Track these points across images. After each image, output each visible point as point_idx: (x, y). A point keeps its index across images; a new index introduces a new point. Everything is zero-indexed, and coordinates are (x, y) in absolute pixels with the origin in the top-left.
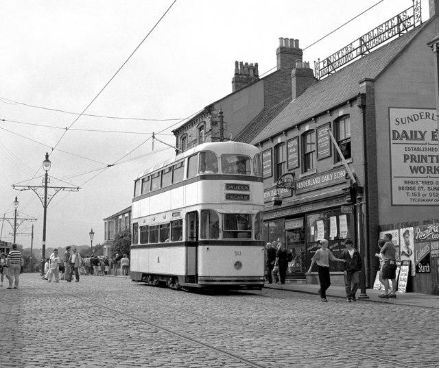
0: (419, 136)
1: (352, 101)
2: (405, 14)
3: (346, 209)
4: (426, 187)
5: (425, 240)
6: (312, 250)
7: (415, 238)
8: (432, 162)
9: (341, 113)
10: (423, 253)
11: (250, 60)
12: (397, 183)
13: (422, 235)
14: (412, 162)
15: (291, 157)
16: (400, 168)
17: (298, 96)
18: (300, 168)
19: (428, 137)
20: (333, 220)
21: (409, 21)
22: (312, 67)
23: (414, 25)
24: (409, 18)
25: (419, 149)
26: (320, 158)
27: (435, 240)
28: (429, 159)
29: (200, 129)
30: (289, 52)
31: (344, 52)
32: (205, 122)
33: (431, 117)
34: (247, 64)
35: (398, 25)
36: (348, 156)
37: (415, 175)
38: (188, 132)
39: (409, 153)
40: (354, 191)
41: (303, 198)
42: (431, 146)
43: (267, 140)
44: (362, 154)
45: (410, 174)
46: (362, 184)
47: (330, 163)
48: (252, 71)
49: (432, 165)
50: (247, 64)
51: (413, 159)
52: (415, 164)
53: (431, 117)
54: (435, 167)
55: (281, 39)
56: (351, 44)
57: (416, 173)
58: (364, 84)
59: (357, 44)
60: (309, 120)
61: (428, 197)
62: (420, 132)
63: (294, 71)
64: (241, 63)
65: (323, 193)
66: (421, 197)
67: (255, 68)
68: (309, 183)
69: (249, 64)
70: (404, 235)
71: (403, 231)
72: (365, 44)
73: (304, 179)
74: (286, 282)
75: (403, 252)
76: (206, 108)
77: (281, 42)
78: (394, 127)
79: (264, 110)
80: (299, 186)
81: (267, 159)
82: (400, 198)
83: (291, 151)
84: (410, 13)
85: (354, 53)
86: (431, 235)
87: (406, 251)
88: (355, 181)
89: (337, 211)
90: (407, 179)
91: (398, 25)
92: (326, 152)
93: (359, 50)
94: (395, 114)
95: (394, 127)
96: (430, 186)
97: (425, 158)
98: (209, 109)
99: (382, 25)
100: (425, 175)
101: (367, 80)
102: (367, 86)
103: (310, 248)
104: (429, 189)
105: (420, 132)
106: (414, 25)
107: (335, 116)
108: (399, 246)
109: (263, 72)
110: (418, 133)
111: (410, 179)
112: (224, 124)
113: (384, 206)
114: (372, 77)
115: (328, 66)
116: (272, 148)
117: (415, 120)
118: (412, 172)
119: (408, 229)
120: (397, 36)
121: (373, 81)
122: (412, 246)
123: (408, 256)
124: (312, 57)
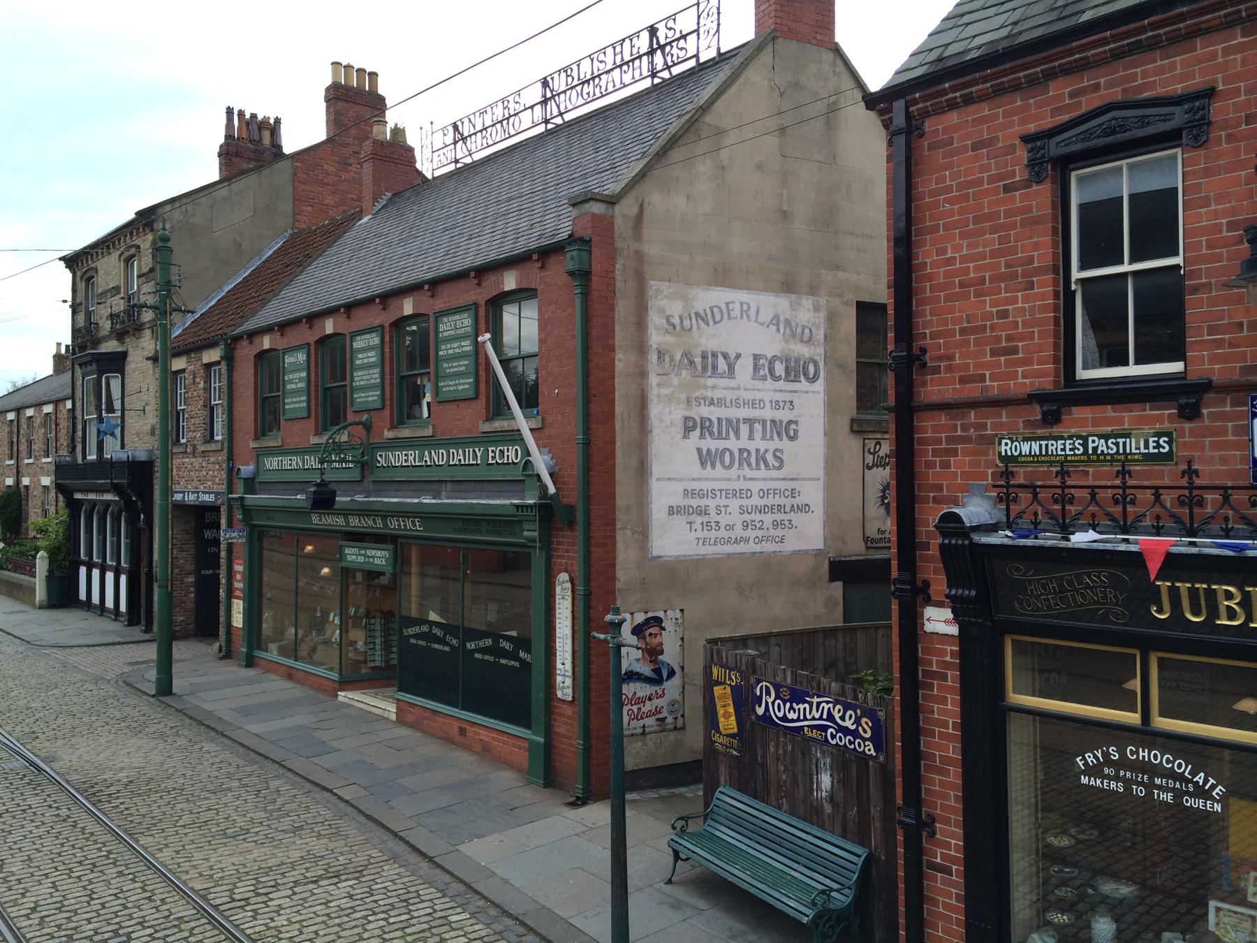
2: (671, 24)
4: (734, 504)
6: (416, 636)
8: (751, 437)
14: (702, 436)
18: (387, 412)
19: (744, 369)
23: (696, 56)
24: (684, 37)
25: (720, 403)
30: (354, 100)
31: (499, 113)
32: (138, 247)
33: (752, 313)
34: (254, 116)
35: (651, 52)
38: (98, 264)
42: (750, 396)
43: (296, 322)
48: (266, 135)
49: (752, 446)
50: (254, 116)
51: (705, 427)
53: (752, 313)
54: (758, 451)
55: (336, 64)
56: (518, 93)
57: (713, 466)
59: (535, 94)
60: (412, 289)
61: (739, 532)
62: (725, 356)
64: (241, 114)
66: (723, 533)
67: (274, 128)
69: (260, 117)
76: (142, 214)
77: (335, 73)
82: (672, 540)
84: (686, 23)
85: (526, 119)
86: (825, 728)
91: (651, 52)
93: (538, 108)
96: (745, 502)
98: (146, 218)
99: (603, 51)
100: (734, 471)
103: (411, 631)
104: (742, 510)
105: (725, 356)
106: (696, 56)
109: (292, 142)
110: (721, 358)
112: (174, 270)
115: (455, 143)
116: (309, 344)
117: (715, 323)
118: (703, 464)
120: (647, 83)
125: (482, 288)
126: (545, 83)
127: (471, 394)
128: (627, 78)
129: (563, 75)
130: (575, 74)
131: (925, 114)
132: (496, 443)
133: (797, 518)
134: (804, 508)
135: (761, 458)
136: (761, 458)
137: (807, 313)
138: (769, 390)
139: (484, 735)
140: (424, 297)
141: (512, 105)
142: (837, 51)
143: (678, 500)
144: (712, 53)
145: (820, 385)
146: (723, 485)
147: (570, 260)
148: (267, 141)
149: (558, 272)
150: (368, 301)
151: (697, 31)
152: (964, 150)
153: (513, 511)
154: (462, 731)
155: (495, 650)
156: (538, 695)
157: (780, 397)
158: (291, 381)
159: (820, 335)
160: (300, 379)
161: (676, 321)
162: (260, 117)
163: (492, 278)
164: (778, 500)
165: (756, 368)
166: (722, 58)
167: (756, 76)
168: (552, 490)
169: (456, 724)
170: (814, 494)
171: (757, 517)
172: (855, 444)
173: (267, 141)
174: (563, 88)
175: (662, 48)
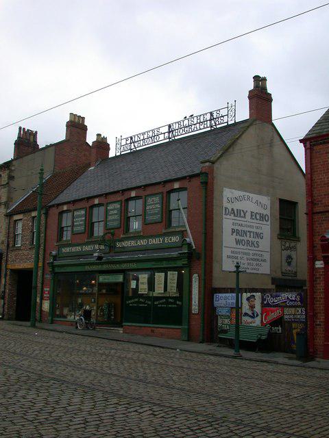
0: (242, 214)
1: (191, 177)
4: (245, 257)
5: (277, 306)
7: (262, 303)
8: (250, 237)
10: (274, 315)
11: (34, 130)
13: (270, 300)
15: (110, 218)
18: (122, 228)
19: (248, 215)
21: (222, 118)
22: (111, 142)
25: (241, 225)
26: (147, 222)
30: (77, 126)
31: (151, 134)
37: (238, 246)
39: (236, 227)
41: (117, 258)
42: (249, 224)
48: (32, 137)
51: (237, 232)
58: (207, 164)
59: (166, 129)
64: (24, 129)
67: (34, 135)
70: (248, 299)
80: (118, 245)
84: (224, 112)
85: (162, 137)
86: (286, 302)
87: (250, 313)
90: (233, 250)
91: (210, 120)
97: (245, 233)
107: (168, 187)
111: (235, 250)
115: (131, 143)
118: (237, 244)
119: (254, 294)
120: (209, 129)
122: (258, 309)
123: (253, 317)
126: (170, 126)
127: (160, 220)
128: (202, 127)
129: (177, 124)
130: (182, 124)
131: (314, 145)
132: (172, 236)
133: (263, 263)
134: (264, 261)
136: (253, 243)
137: (265, 200)
138: (255, 223)
139: (161, 330)
140: (71, 205)
141: (156, 132)
142: (273, 125)
143: (230, 254)
144: (233, 122)
145: (269, 223)
146: (243, 251)
147: (202, 179)
148: (32, 140)
149: (196, 182)
150: (118, 192)
151: (227, 115)
152: (323, 154)
153: (179, 255)
154: (152, 331)
155: (167, 303)
156: (185, 312)
157: (258, 225)
158: (81, 221)
159: (269, 207)
160: (81, 221)
161: (230, 199)
162: (51, 133)
163: (126, 193)
164: (258, 257)
165: (252, 216)
166: (236, 124)
167: (252, 131)
169: (150, 329)
170: (267, 256)
172: (279, 241)
173: (32, 140)
174: (177, 128)
175: (214, 119)
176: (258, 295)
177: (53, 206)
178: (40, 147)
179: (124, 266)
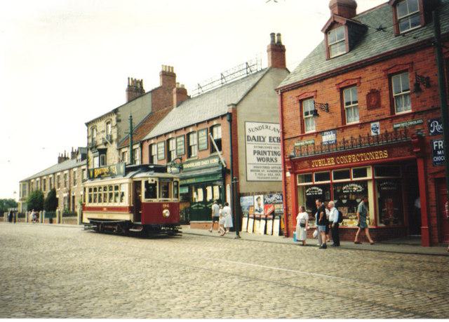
0: (262, 139)
1: (223, 116)
3: (219, 183)
9: (215, 123)
10: (270, 210)
11: (138, 78)
12: (250, 167)
13: (268, 200)
15: (178, 148)
16: (252, 159)
17: (178, 106)
19: (267, 140)
20: (209, 189)
27: (277, 204)
28: (268, 153)
29: (107, 123)
30: (168, 76)
36: (220, 149)
39: (256, 149)
40: (225, 172)
41: (188, 174)
44: (229, 150)
45: (256, 162)
46: (229, 167)
47: (208, 153)
48: (139, 84)
51: (259, 153)
52: (259, 156)
55: (163, 66)
58: (231, 107)
60: (193, 125)
61: (267, 176)
63: (175, 90)
65: (203, 172)
67: (141, 83)
68: (192, 165)
70: (257, 200)
71: (256, 197)
72: (224, 78)
73: (188, 162)
74: (342, 243)
75: (256, 210)
78: (248, 133)
79: (151, 113)
80: (185, 166)
81: (161, 147)
82: (252, 176)
83: (179, 144)
84: (254, 63)
88: (225, 166)
89: (212, 184)
92: (205, 146)
94: (249, 125)
95: (248, 133)
97: (265, 153)
98: (116, 111)
100: (265, 163)
101: (233, 104)
102: (233, 108)
108: (253, 206)
109: (147, 87)
113: (242, 182)
114: (235, 102)
121: (236, 105)
122: (262, 207)
123: (260, 212)
124: (181, 80)
125: (209, 124)
135: (272, 160)
148: (139, 87)
149: (226, 119)
165: (270, 139)
166: (262, 70)
168: (225, 166)
171: (272, 173)
173: (139, 87)
176: (262, 196)
177: (145, 141)
178: (146, 92)
179: (189, 181)
